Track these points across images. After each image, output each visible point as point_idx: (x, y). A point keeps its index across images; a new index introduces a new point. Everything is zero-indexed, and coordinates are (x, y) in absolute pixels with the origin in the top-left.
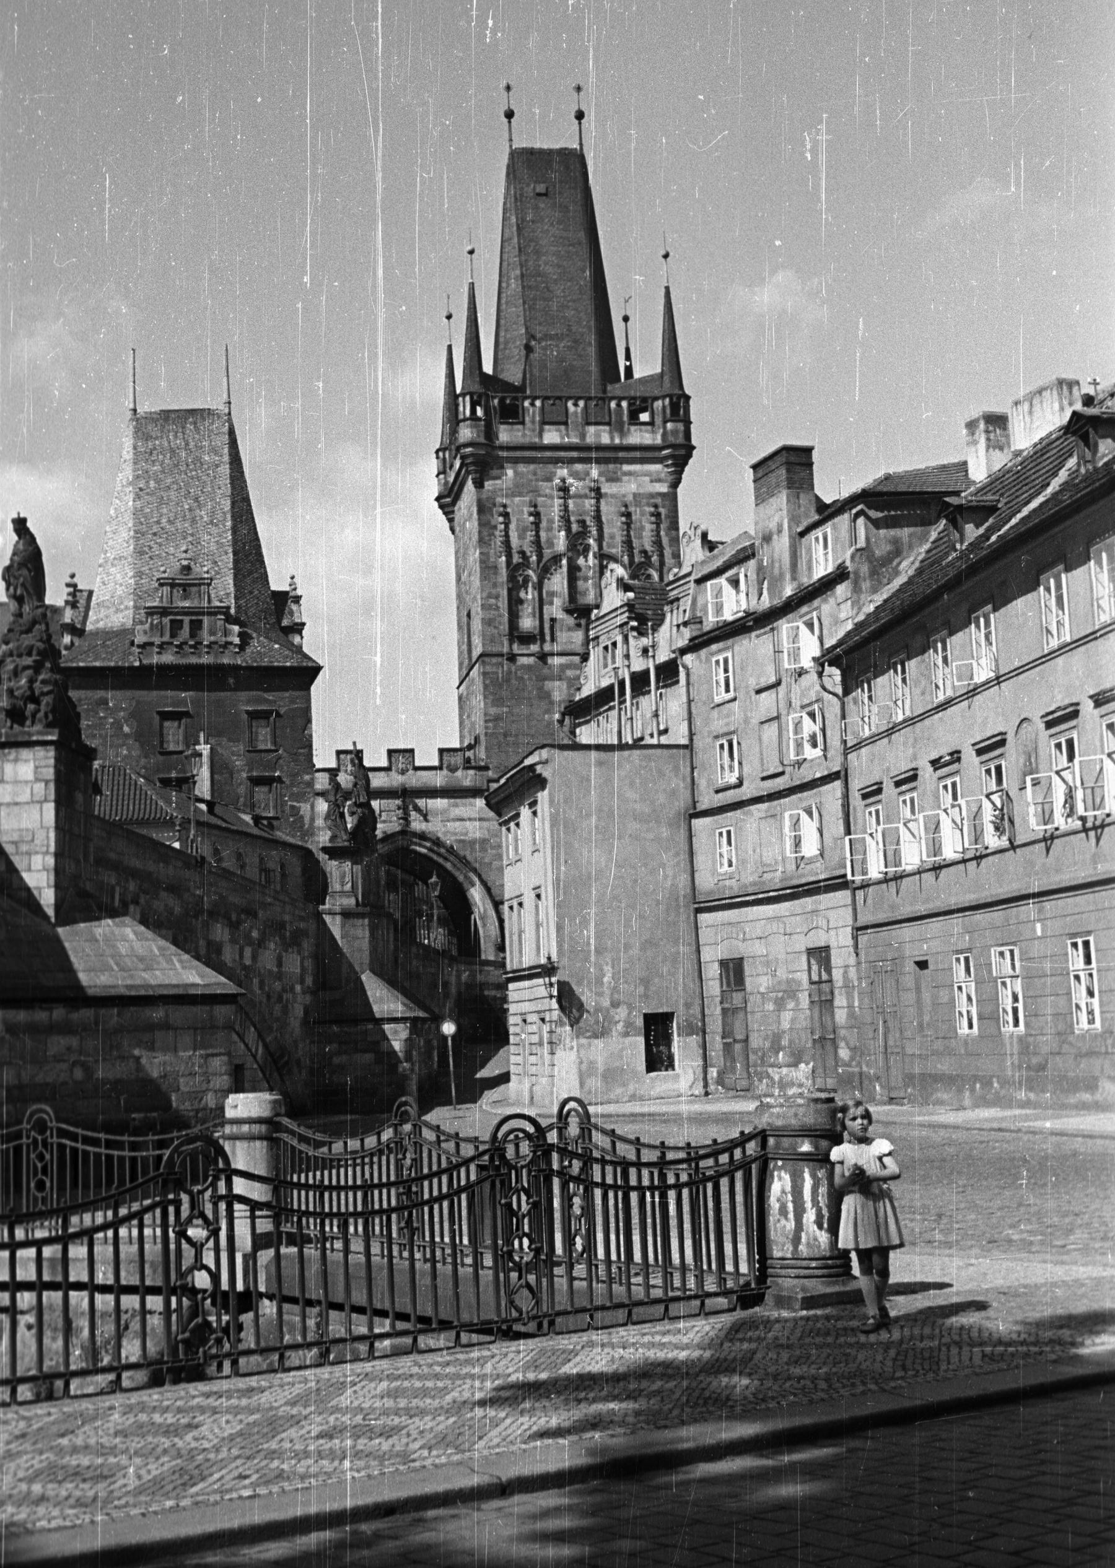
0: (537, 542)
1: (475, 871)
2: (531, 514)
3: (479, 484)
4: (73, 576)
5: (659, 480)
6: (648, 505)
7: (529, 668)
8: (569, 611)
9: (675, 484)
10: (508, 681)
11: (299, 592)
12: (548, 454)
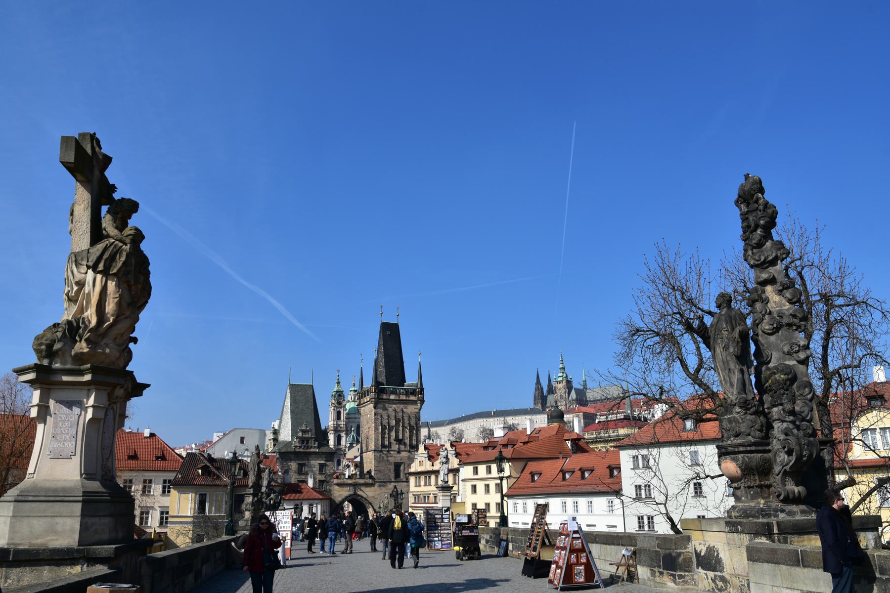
3: (375, 408)
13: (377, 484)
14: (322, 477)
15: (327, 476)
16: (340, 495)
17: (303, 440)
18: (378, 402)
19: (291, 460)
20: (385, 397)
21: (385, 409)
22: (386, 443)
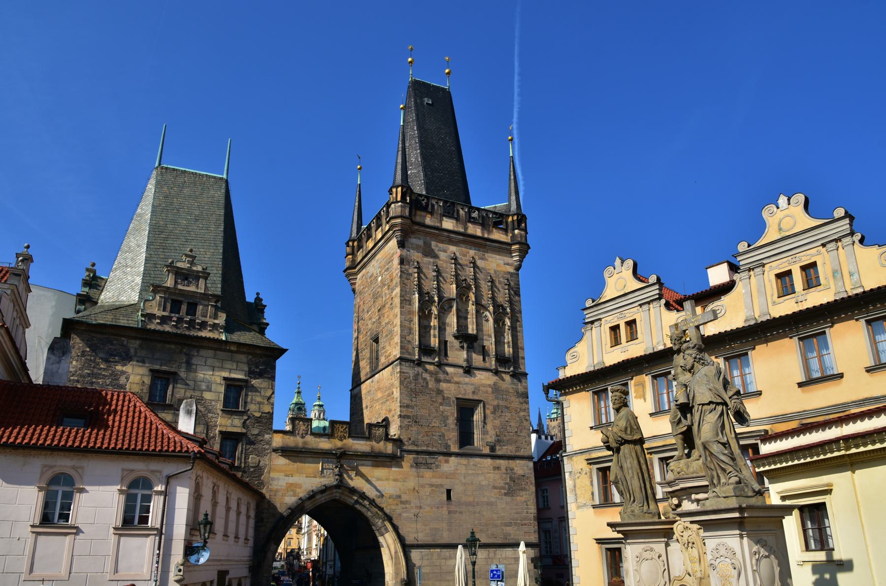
0: (439, 288)
1: (390, 519)
2: (434, 271)
3: (401, 245)
4: (94, 265)
5: (508, 264)
6: (503, 277)
7: (431, 373)
8: (456, 337)
9: (518, 268)
10: (416, 380)
11: (264, 303)
12: (446, 234)
13: (409, 459)
14: (234, 424)
15: (249, 419)
16: (291, 487)
17: (175, 301)
18: (409, 232)
19: (126, 358)
20: (428, 221)
21: (429, 252)
22: (434, 342)
